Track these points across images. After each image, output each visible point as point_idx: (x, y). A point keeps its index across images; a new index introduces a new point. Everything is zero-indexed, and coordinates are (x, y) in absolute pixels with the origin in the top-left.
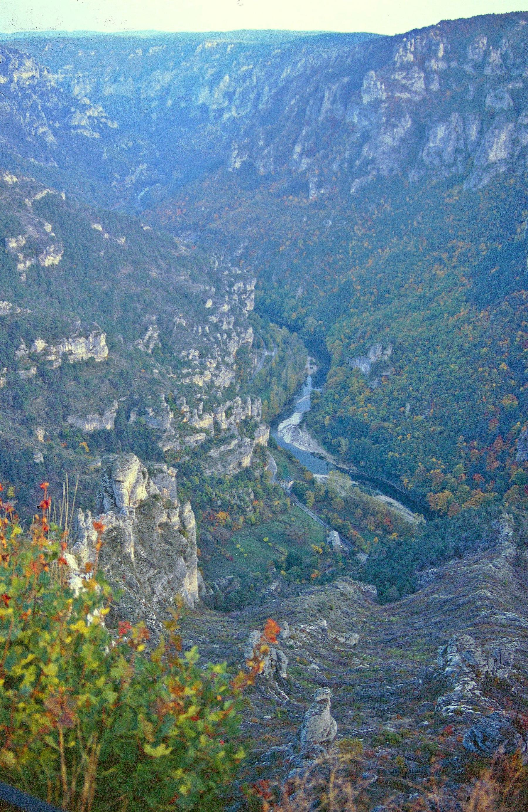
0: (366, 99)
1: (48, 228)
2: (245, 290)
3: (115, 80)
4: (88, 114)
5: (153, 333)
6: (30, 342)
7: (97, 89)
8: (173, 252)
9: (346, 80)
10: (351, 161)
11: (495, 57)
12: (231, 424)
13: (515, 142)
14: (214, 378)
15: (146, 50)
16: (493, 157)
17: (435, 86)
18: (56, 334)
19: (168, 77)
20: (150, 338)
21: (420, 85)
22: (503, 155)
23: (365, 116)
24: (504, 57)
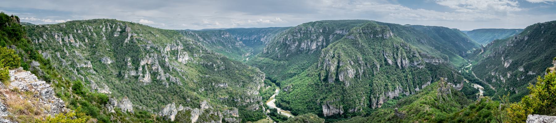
5: (241, 83)
6: (212, 83)
13: (317, 45)
16: (313, 48)
18: (218, 82)
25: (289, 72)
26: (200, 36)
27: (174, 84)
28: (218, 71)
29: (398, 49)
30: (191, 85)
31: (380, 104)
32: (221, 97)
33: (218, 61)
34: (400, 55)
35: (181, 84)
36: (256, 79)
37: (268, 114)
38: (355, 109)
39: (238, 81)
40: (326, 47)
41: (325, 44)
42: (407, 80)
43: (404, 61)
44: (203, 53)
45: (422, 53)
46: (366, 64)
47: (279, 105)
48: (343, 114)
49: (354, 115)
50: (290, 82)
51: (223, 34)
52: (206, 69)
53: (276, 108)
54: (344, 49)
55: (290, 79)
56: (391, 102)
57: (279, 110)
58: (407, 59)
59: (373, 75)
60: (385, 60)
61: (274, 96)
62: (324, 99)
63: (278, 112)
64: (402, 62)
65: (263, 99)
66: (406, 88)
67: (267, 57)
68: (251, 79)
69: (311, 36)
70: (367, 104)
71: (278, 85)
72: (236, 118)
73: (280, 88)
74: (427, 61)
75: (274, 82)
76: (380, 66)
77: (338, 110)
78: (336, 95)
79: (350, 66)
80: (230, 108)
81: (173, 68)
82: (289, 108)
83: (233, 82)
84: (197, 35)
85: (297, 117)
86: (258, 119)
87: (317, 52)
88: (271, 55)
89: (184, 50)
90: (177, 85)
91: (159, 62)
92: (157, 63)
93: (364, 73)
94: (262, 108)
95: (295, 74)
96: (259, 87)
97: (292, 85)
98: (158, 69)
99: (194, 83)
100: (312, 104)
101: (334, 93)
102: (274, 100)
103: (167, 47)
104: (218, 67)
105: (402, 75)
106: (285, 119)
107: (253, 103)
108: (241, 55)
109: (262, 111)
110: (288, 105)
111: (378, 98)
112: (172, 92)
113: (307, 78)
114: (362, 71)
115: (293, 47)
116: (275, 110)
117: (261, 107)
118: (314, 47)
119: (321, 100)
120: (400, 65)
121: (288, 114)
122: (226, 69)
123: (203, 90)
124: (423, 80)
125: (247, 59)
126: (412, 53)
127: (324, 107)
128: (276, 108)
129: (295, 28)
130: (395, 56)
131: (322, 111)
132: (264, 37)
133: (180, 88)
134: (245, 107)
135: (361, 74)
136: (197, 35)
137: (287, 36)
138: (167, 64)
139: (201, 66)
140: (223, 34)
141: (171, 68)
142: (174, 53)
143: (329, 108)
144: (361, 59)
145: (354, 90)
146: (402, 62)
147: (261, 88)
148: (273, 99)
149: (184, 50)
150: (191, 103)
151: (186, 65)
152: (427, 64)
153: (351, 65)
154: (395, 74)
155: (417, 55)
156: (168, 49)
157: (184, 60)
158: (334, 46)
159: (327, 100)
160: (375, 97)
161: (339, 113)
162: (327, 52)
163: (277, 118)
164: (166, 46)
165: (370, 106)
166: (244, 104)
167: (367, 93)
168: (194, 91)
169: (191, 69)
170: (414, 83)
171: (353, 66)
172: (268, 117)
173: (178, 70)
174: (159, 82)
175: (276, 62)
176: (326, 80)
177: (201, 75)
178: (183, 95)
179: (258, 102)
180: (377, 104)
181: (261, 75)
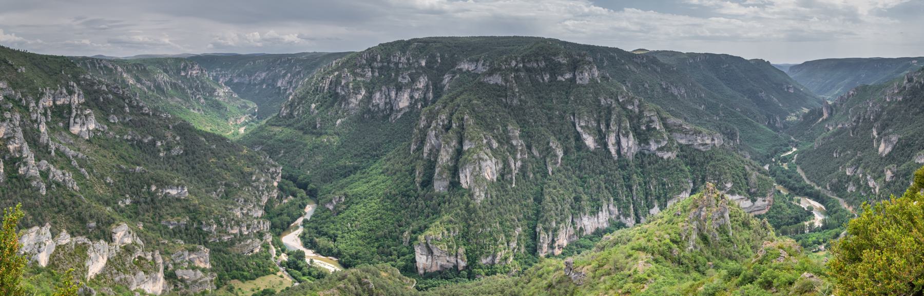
0: (343, 82)
1: (178, 138)
5: (222, 189)
6: (149, 186)
9: (336, 73)
10: (337, 112)
11: (403, 59)
13: (412, 97)
16: (401, 105)
17: (377, 74)
18: (163, 184)
21: (370, 74)
22: (407, 104)
24: (408, 59)
26: (129, 71)
27: (58, 185)
28: (168, 158)
29: (609, 110)
30: (100, 190)
31: (560, 247)
32: (169, 219)
33: (169, 135)
34: (614, 127)
35: (76, 187)
36: (258, 180)
37: (282, 265)
38: (494, 257)
39: (214, 184)
40: (434, 102)
41: (431, 95)
42: (630, 187)
43: (624, 141)
44: (131, 113)
45: (672, 120)
46: (529, 147)
47: (309, 243)
48: (467, 267)
49: (492, 271)
50: (342, 187)
51: (184, 69)
52: (138, 151)
53: (302, 249)
54: (473, 112)
55: (343, 181)
56: (587, 242)
57: (309, 253)
58: (631, 136)
59: (545, 174)
60: (578, 138)
61: (300, 221)
62: (421, 230)
63: (308, 261)
64: (618, 143)
65: (273, 227)
66: (627, 208)
67: (289, 126)
68: (245, 179)
69: (397, 75)
70: (527, 247)
71: (313, 194)
72: (203, 270)
73: (317, 203)
74: (683, 142)
75: (304, 186)
76: (565, 153)
77: (453, 260)
78: (451, 222)
79: (488, 151)
80: (191, 246)
81: (57, 150)
82: (335, 251)
83: (201, 185)
84: (120, 69)
86: (257, 276)
87: (411, 115)
88: (298, 121)
89: (86, 105)
90: (65, 188)
91: (25, 132)
92: (20, 134)
93: (523, 170)
94: (268, 248)
95: (356, 169)
96: (265, 200)
97: (346, 196)
98: (20, 150)
99: (108, 185)
100: (389, 242)
101: (446, 217)
102: (300, 230)
103: (45, 98)
104: (168, 148)
105: (618, 174)
106: (321, 275)
107: (248, 237)
109: (268, 257)
110: (331, 244)
111: (555, 230)
112: (53, 206)
113: (382, 177)
114: (519, 164)
115: (354, 101)
116: (300, 255)
117: (266, 247)
118: (404, 102)
119: (414, 232)
120: (613, 150)
121: (330, 266)
122: (186, 153)
123: (128, 202)
124: (671, 189)
126: (644, 120)
127: (418, 250)
128: (302, 249)
129: (360, 54)
130: (603, 127)
131: (414, 261)
132: (284, 76)
133: (72, 196)
134: (226, 244)
135: (515, 172)
136: (120, 69)
137: (339, 76)
138: (44, 138)
139: (126, 145)
140: (184, 69)
141: (53, 147)
142: (61, 114)
143: (430, 252)
144: (517, 133)
145: (494, 212)
146: (618, 143)
147: (270, 201)
148: (297, 227)
149: (86, 105)
150: (97, 232)
151: (89, 141)
152: (681, 147)
153: (491, 148)
154: (601, 173)
155: (658, 126)
156: (47, 102)
157: (85, 129)
158: (452, 101)
159: (428, 233)
160: (546, 230)
161: (456, 267)
162: (432, 116)
163: (304, 275)
164: (42, 94)
165: (533, 250)
166: (226, 238)
167: (529, 218)
168: (107, 203)
169: (102, 151)
170: (647, 195)
171: (495, 152)
172: (282, 271)
173: (70, 152)
174: (24, 181)
176: (427, 183)
177: (124, 167)
178: (79, 214)
179: (260, 235)
180: (551, 246)
181: (272, 169)
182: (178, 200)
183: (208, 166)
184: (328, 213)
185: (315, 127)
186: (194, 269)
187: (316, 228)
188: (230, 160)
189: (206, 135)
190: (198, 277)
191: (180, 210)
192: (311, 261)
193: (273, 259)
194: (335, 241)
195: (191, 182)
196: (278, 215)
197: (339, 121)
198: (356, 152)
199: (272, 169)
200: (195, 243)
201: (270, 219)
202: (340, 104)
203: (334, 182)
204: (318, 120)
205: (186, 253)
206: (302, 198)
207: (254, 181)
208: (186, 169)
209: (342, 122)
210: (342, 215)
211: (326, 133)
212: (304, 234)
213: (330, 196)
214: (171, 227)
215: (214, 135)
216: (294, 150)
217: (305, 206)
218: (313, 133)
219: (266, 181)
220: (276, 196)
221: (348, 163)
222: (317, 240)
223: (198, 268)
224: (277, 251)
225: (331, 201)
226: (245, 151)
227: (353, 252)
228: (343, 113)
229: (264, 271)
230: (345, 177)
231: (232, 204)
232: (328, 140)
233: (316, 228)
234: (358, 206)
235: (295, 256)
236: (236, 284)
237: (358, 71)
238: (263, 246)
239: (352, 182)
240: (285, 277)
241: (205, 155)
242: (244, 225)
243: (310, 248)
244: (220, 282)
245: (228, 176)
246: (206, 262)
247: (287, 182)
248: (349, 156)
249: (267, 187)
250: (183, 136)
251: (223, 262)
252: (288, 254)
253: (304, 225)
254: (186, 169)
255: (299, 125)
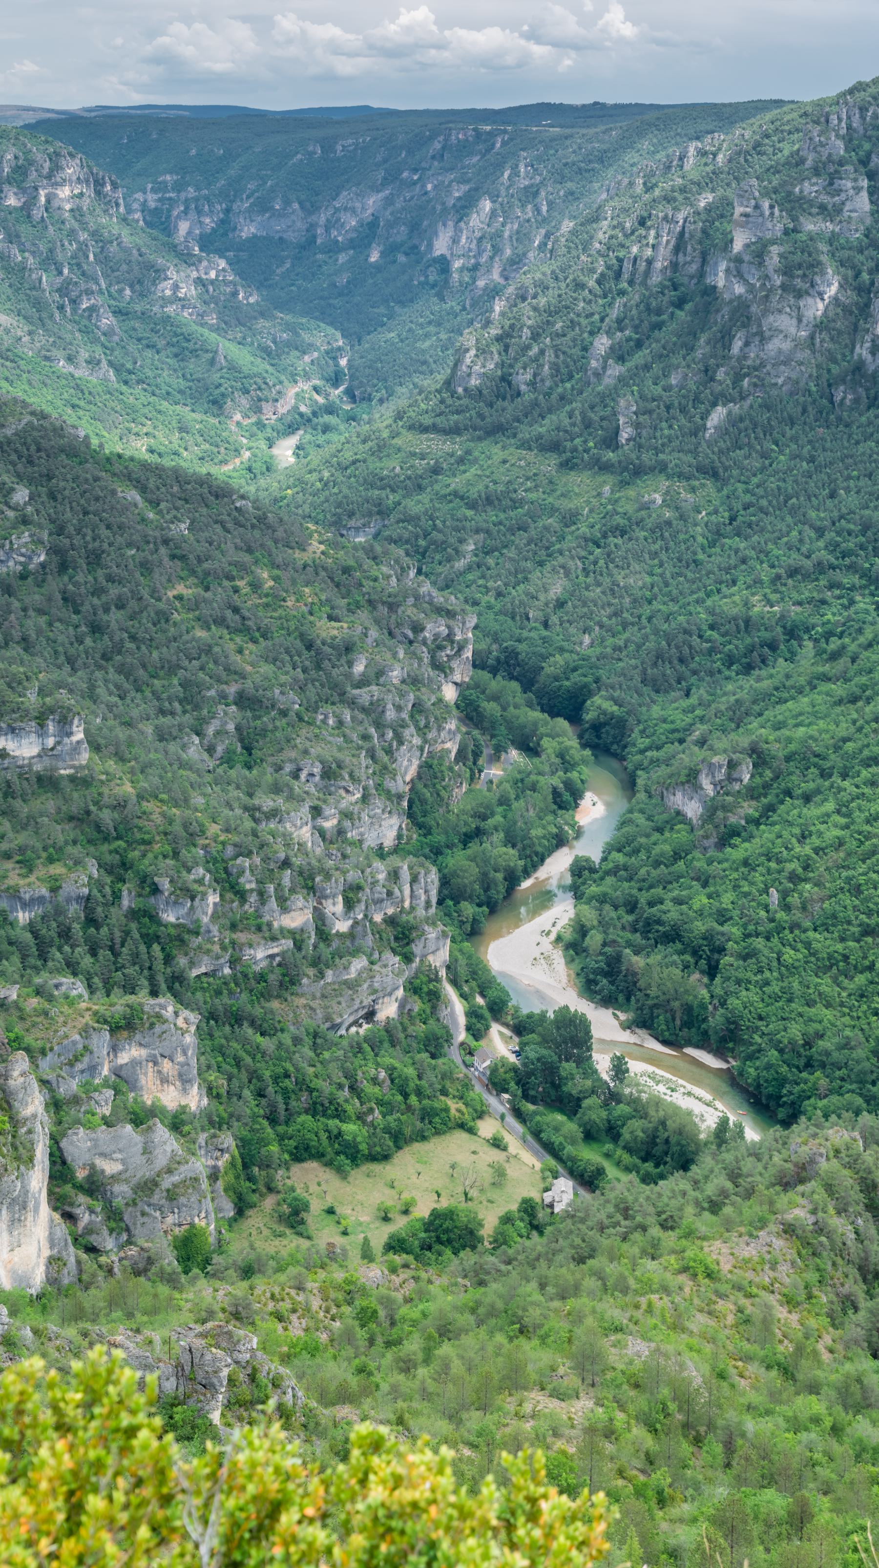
2: (450, 637)
3: (262, 206)
4: (195, 274)
5: (227, 719)
7: (226, 225)
8: (297, 554)
9: (705, 199)
12: (356, 923)
14: (347, 824)
15: (328, 146)
19: (372, 202)
20: (218, 733)
23: (740, 275)
25: (730, 603)
39: (191, 697)
47: (607, 980)
50: (738, 716)
61: (557, 867)
65: (450, 893)
68: (321, 666)
71: (606, 742)
73: (629, 785)
75: (568, 705)
80: (119, 1004)
83: (139, 706)
85: (802, 1140)
94: (434, 998)
95: (793, 632)
102: (562, 913)
108: (217, 405)
116: (572, 1036)
125: (285, 452)
129: (818, 115)
137: (720, 211)
147: (429, 771)
163: (589, 1136)
175: (586, 493)
181: (434, 628)
182: (47, 782)
183: (163, 617)
184: (680, 835)
185: (611, 441)
186: (140, 1118)
187: (632, 906)
188: (255, 586)
189: (148, 478)
190: (161, 1161)
191: (60, 833)
192: (619, 1069)
193: (455, 1055)
194: (712, 971)
195: (91, 695)
196: (467, 839)
197: (718, 416)
198: (795, 559)
199: (434, 628)
200: (130, 988)
201: (436, 853)
202: (725, 339)
203: (700, 693)
204: (627, 406)
205: (102, 1041)
206: (565, 762)
207: (362, 683)
208: (63, 634)
209: (733, 421)
210: (740, 850)
211: (662, 468)
212: (582, 930)
213: (688, 756)
214: (23, 917)
215: (179, 477)
216: (520, 539)
217: (576, 795)
218: (605, 468)
219: (413, 681)
220: (452, 747)
221: (758, 608)
222: (638, 961)
223: (154, 1112)
224: (473, 1014)
225: (691, 779)
226: (316, 547)
227: (795, 1031)
228: (737, 378)
229: (427, 1115)
230: (748, 669)
231: (276, 789)
232: (671, 501)
233: (632, 906)
234: (813, 811)
235: (545, 1041)
236: (311, 1181)
237: (810, 188)
238: (413, 988)
239: (779, 694)
240: (514, 1145)
241: (146, 567)
242: (335, 886)
243: (607, 1001)
244: (248, 1181)
245: (252, 663)
246: (185, 1081)
247: (496, 684)
248: (765, 573)
249: (418, 707)
250: (43, 481)
251: (254, 1075)
252: (520, 1029)
253: (576, 892)
254: (63, 634)
255: (544, 427)
